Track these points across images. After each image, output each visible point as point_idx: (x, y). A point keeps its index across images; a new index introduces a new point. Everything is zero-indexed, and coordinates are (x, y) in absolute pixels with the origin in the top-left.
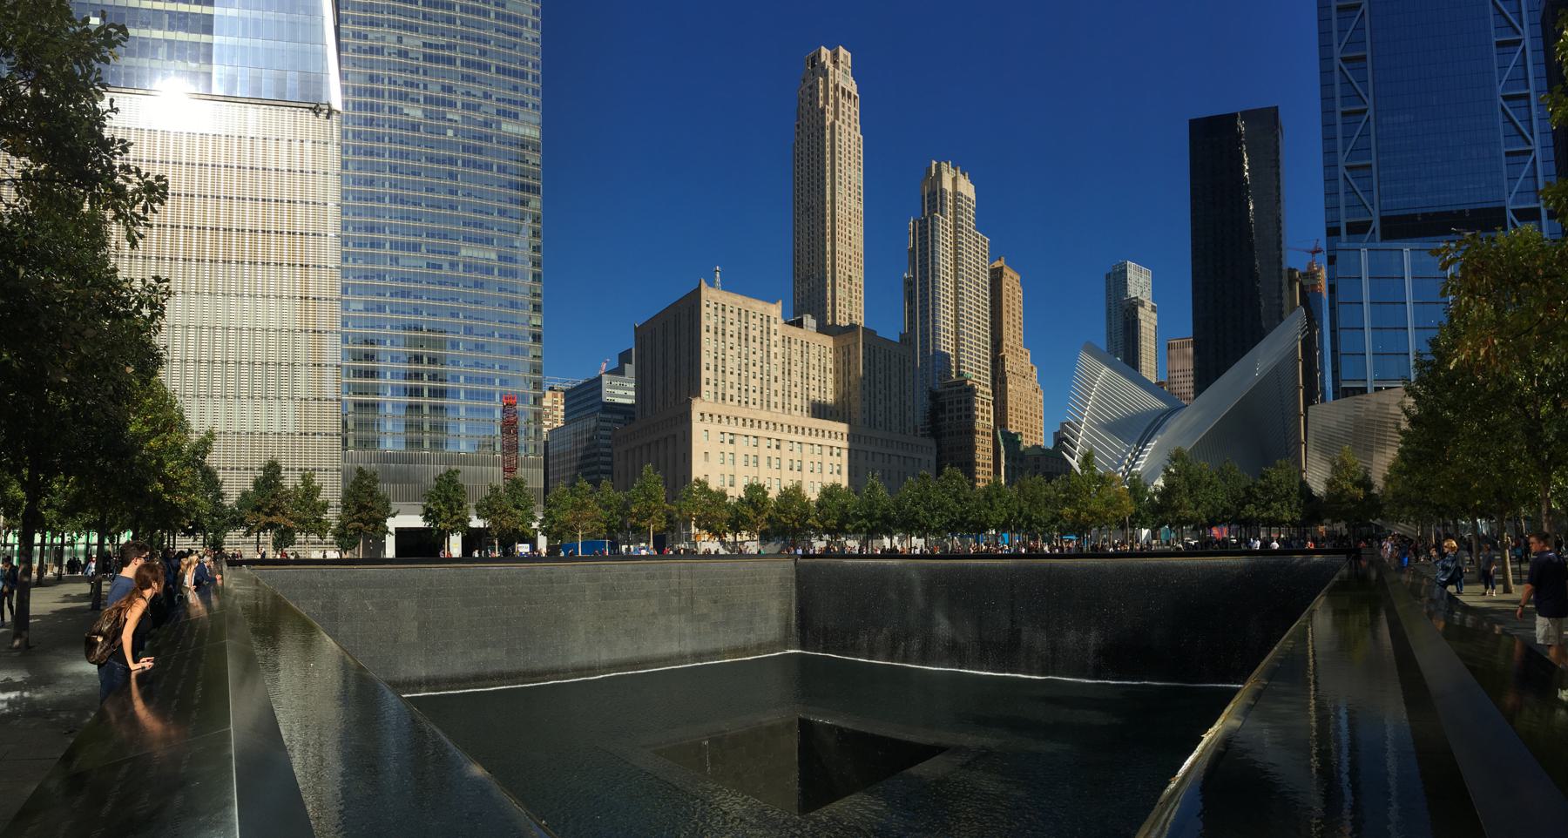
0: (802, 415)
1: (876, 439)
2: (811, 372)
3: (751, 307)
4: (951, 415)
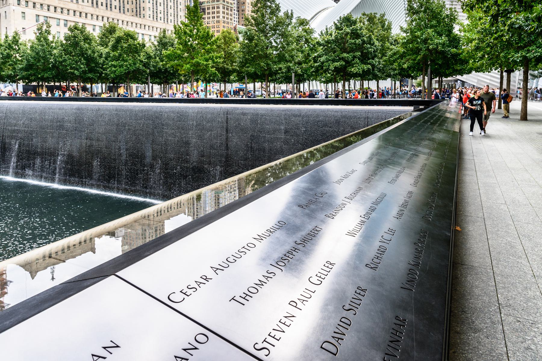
0: (107, 9)
4: (209, 16)
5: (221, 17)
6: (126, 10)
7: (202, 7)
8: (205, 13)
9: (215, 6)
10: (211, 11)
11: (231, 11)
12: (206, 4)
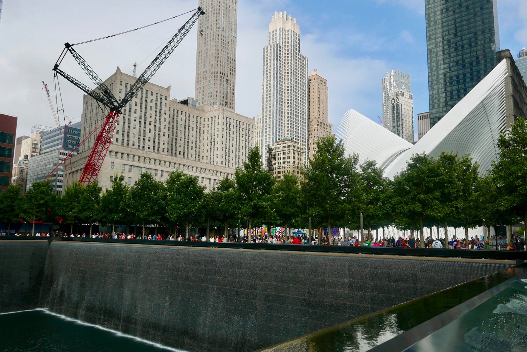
0: (184, 157)
2: (191, 132)
3: (150, 89)
4: (279, 161)
5: (291, 162)
6: (201, 157)
7: (273, 153)
8: (276, 159)
9: (286, 152)
10: (282, 156)
12: (277, 150)
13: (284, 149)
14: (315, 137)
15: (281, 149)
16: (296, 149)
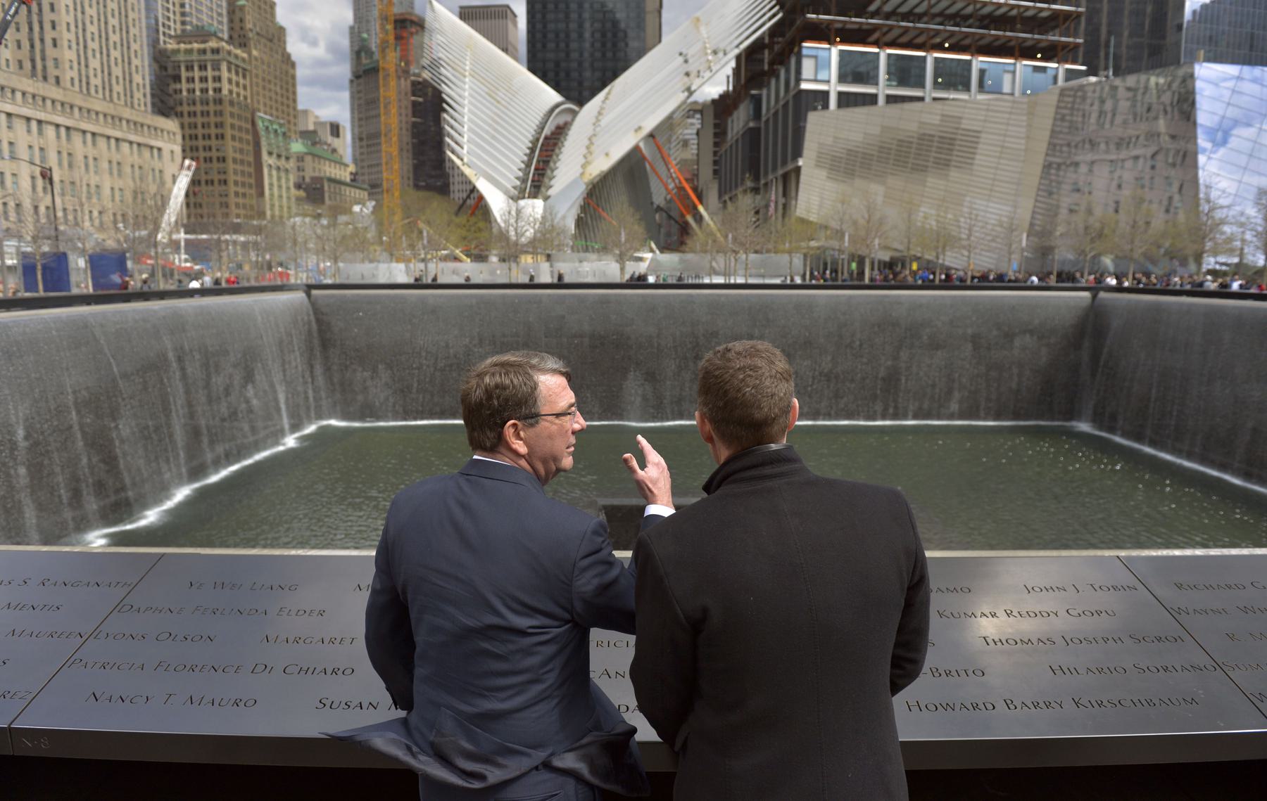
1: (97, 113)
10: (197, 74)
11: (244, 77)
13: (203, 57)
14: (242, 28)
15: (195, 57)
16: (232, 59)
